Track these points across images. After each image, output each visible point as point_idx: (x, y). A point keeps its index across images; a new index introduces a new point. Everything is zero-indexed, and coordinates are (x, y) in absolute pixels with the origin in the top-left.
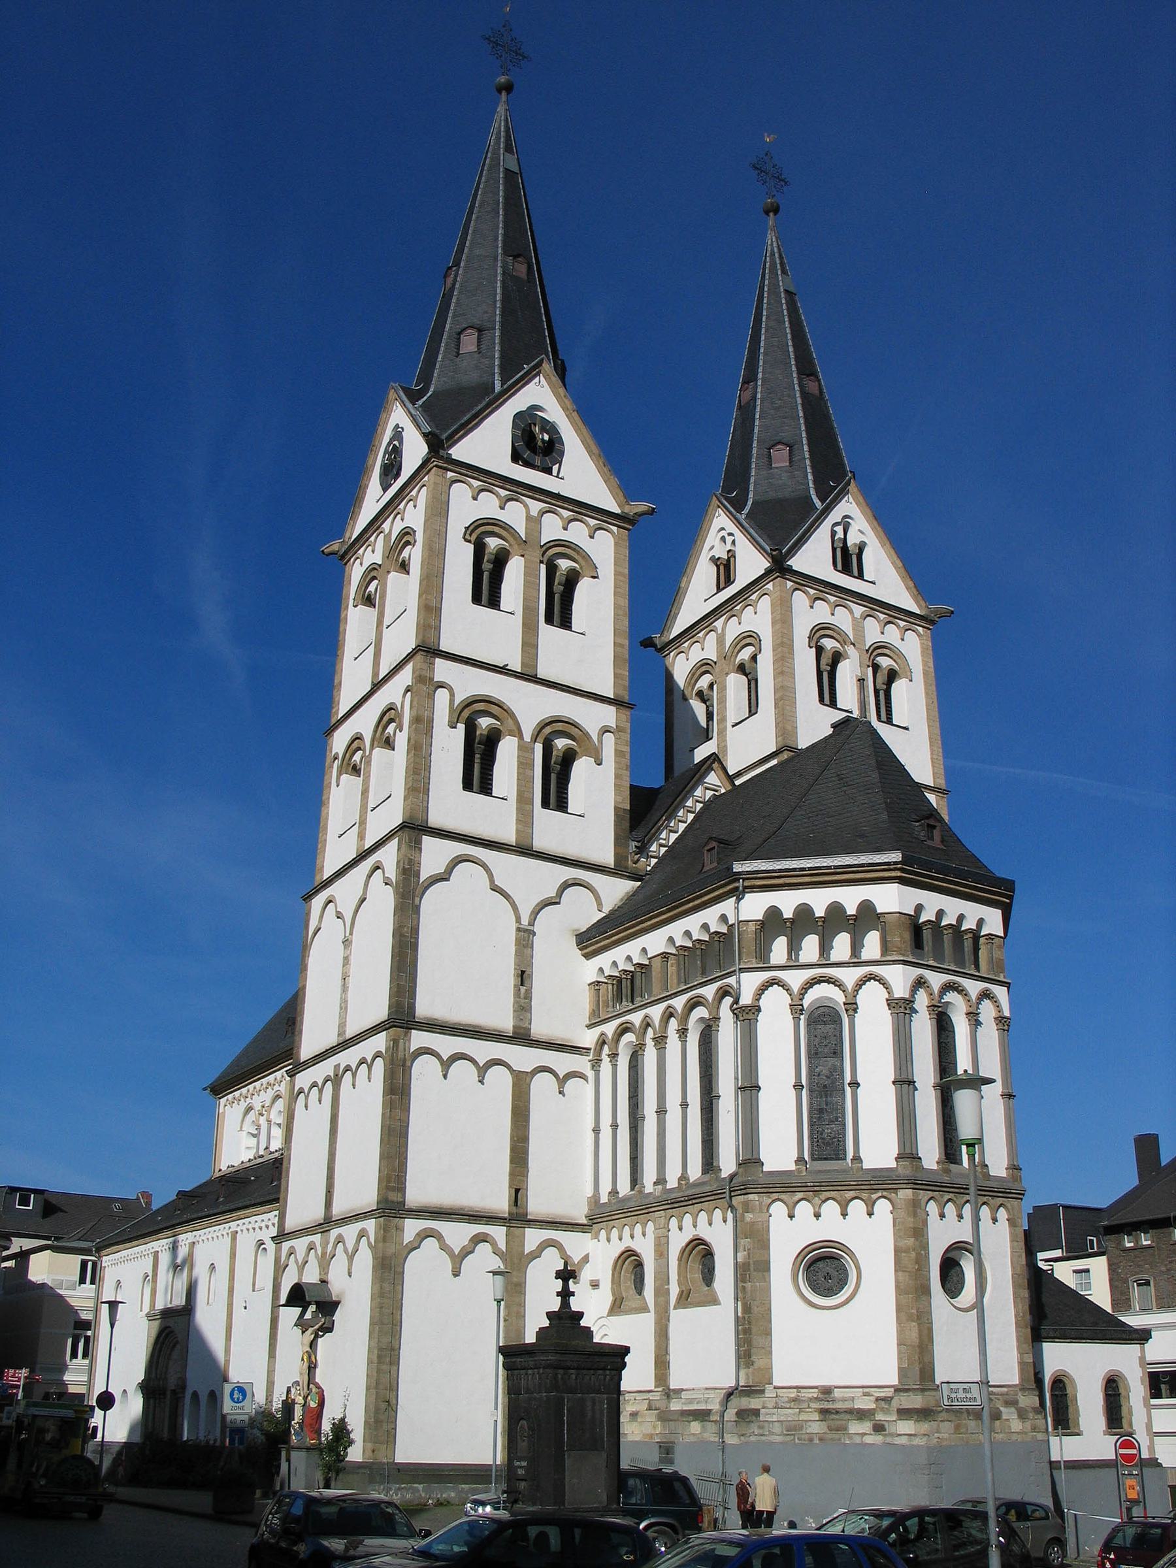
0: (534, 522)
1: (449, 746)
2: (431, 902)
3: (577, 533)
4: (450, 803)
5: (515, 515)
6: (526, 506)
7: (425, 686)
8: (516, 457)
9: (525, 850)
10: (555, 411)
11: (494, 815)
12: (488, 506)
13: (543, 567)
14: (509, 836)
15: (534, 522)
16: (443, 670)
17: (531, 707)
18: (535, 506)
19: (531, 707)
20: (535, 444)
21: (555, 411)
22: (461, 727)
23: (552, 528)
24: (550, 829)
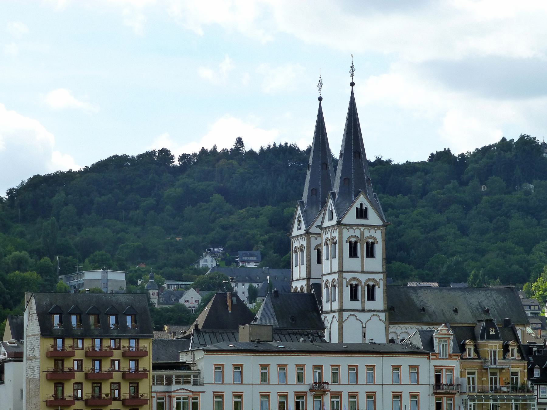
0: (362, 234)
1: (347, 291)
2: (345, 325)
3: (372, 233)
4: (348, 304)
5: (357, 233)
6: (360, 230)
7: (341, 279)
8: (357, 217)
9: (363, 311)
10: (366, 204)
11: (357, 305)
12: (351, 232)
13: (365, 245)
14: (360, 308)
15: (362, 234)
16: (344, 275)
17: (364, 278)
18: (362, 228)
19: (364, 278)
20: (362, 213)
21: (366, 204)
22: (349, 286)
23: (366, 233)
24: (369, 305)
